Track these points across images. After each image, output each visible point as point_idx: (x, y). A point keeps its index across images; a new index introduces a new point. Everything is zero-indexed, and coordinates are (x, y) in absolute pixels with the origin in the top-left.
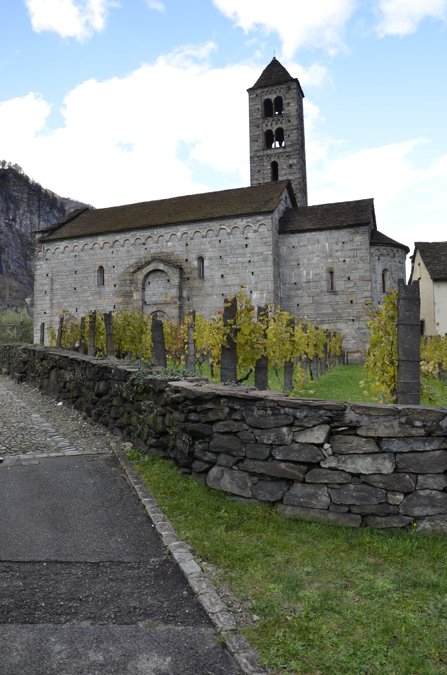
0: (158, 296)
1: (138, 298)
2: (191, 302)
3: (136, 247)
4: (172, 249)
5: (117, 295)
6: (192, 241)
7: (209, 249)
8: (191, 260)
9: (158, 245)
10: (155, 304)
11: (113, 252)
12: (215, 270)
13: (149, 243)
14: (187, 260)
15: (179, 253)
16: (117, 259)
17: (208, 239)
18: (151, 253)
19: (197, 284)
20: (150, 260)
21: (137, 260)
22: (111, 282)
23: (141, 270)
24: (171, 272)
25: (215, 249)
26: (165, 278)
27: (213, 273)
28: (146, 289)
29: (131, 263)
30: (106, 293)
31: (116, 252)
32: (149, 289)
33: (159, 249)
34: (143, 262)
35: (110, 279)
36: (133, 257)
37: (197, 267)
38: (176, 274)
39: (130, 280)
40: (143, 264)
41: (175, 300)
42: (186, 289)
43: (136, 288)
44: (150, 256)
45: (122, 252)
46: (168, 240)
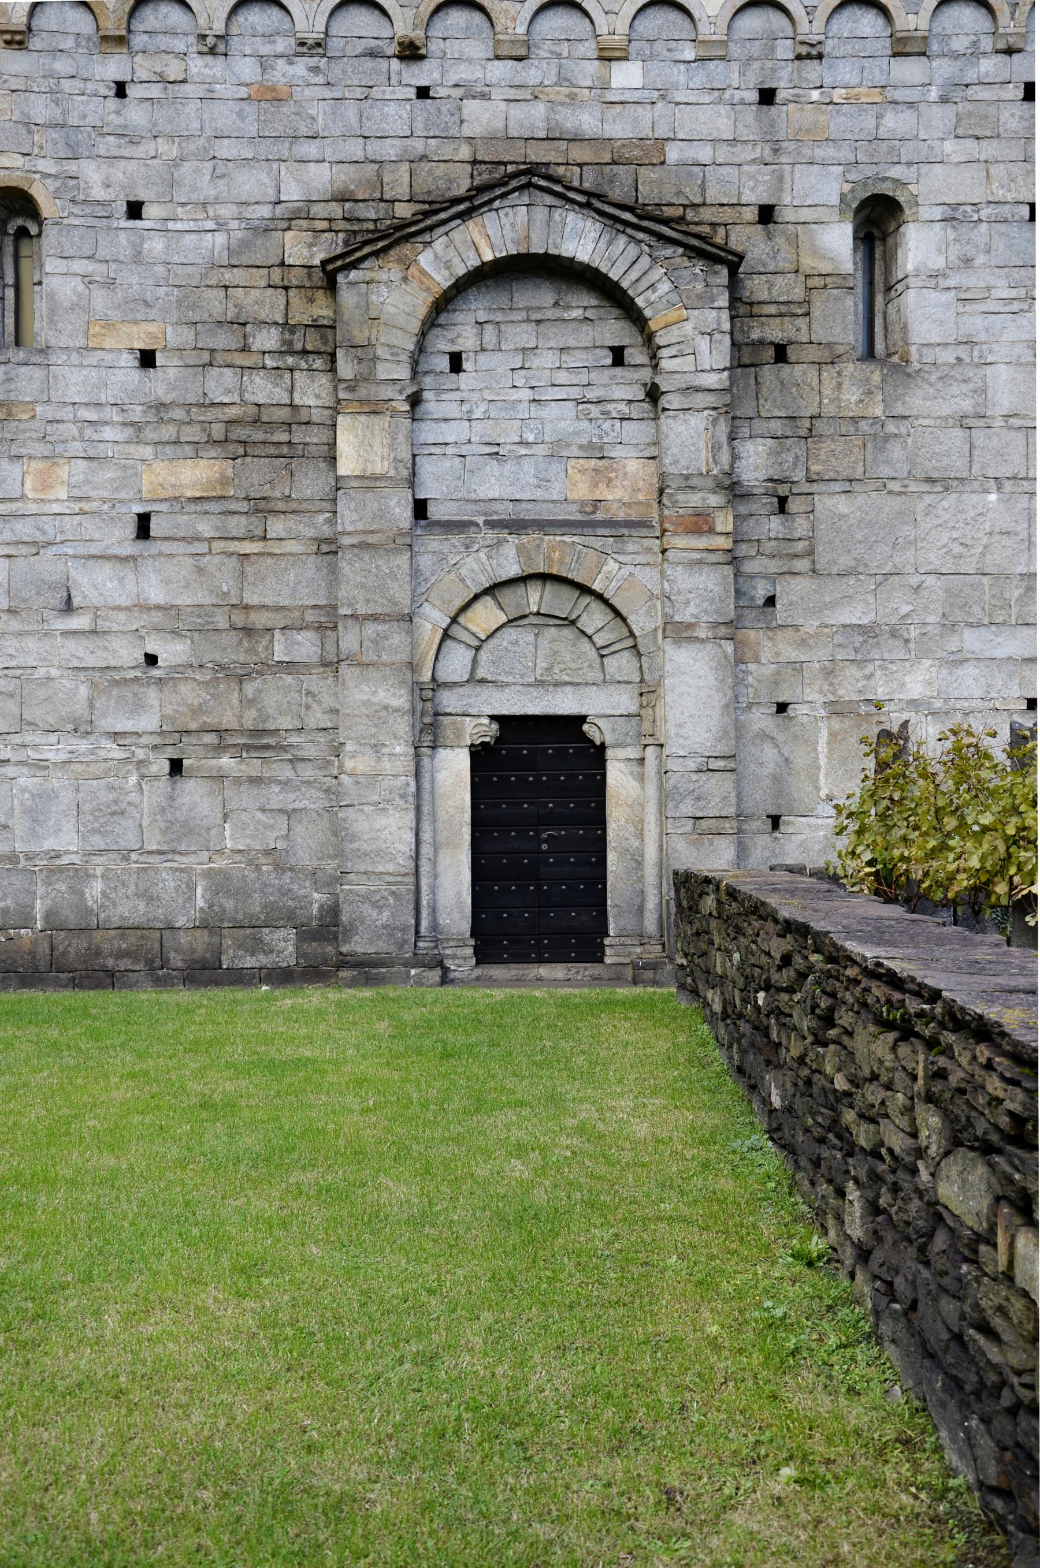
0: (528, 466)
1: (380, 467)
2: (801, 526)
3: (336, 71)
4: (645, 114)
5: (168, 432)
6: (812, 70)
7: (949, 146)
8: (805, 214)
9: (532, 73)
10: (516, 526)
11: (121, 90)
12: (991, 306)
13: (453, 48)
14: (766, 214)
15: (704, 153)
16: (169, 150)
17: (943, 69)
18: (467, 131)
19: (851, 395)
20: (462, 187)
21: (344, 177)
22: (109, 325)
23: (406, 249)
24: (665, 287)
25: (988, 150)
26: (586, 335)
27: (975, 324)
28: (431, 405)
29: (292, 193)
30: (67, 413)
31: (155, 91)
32: (450, 409)
33: (539, 111)
34: (403, 192)
35: (100, 299)
36: (311, 149)
37: (848, 267)
38: (704, 301)
39: (287, 326)
40: (404, 211)
41: (695, 499)
42: (759, 426)
43: (363, 392)
44: (465, 152)
45: (209, 98)
46: (618, 40)
